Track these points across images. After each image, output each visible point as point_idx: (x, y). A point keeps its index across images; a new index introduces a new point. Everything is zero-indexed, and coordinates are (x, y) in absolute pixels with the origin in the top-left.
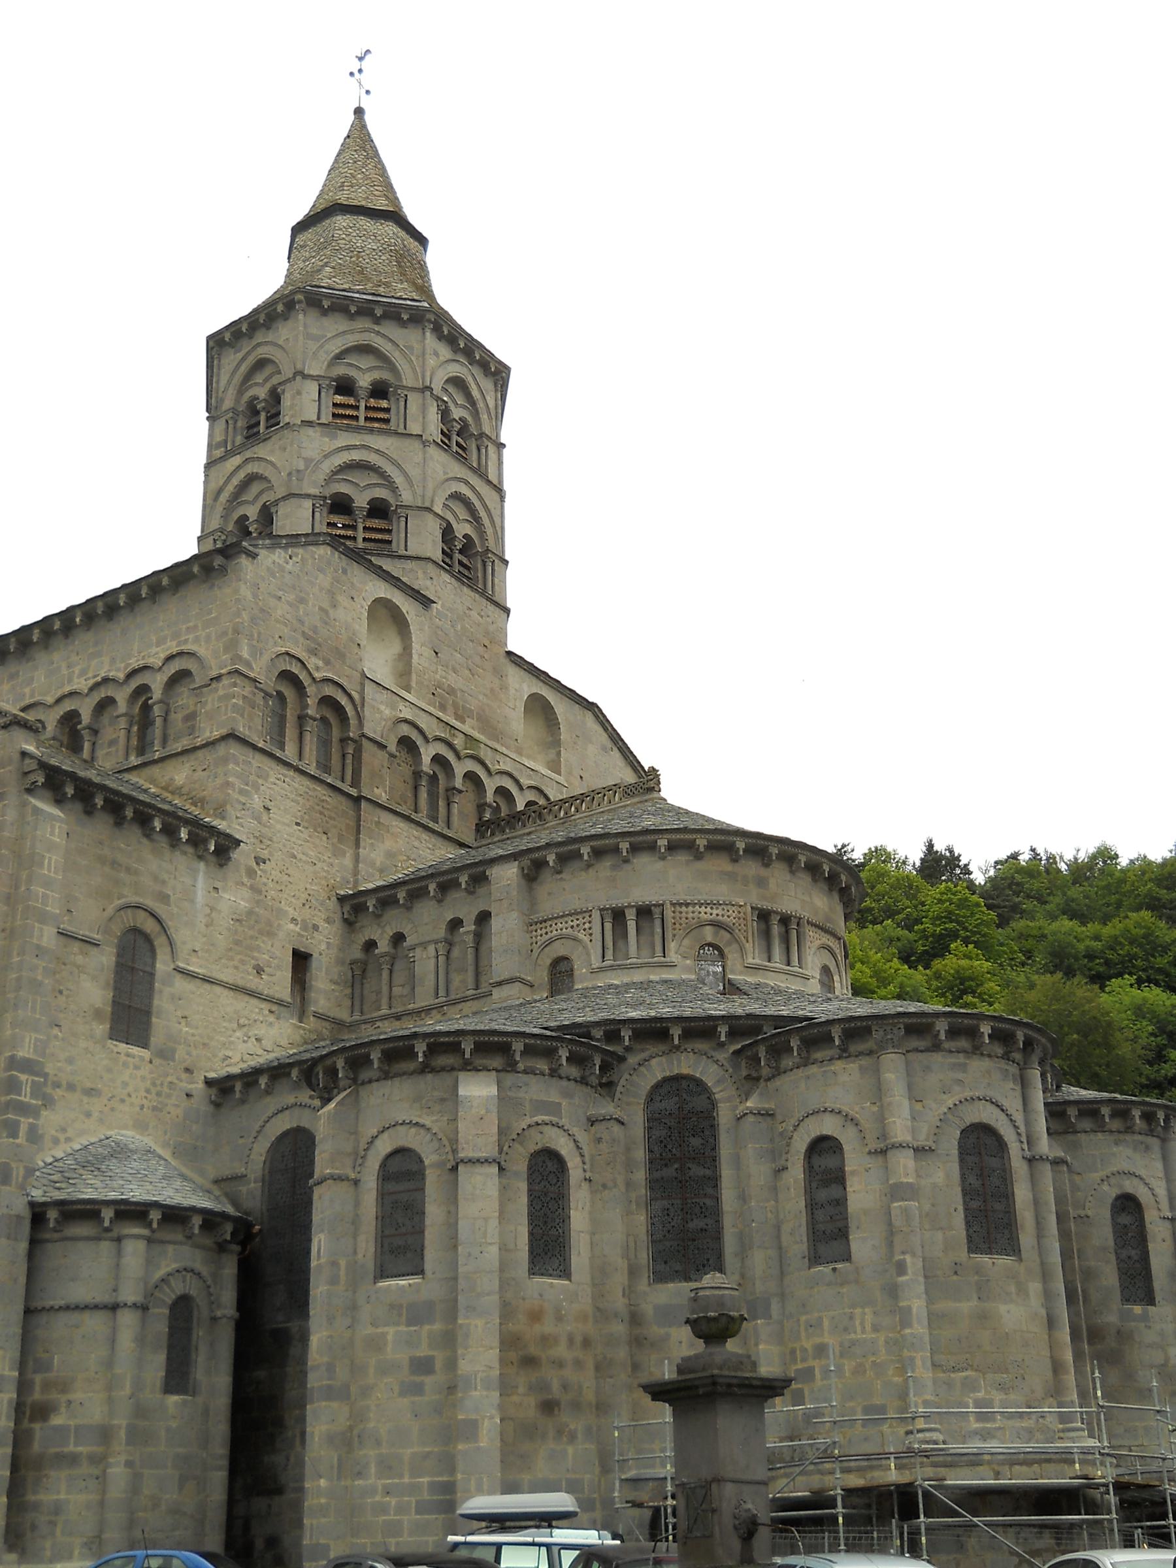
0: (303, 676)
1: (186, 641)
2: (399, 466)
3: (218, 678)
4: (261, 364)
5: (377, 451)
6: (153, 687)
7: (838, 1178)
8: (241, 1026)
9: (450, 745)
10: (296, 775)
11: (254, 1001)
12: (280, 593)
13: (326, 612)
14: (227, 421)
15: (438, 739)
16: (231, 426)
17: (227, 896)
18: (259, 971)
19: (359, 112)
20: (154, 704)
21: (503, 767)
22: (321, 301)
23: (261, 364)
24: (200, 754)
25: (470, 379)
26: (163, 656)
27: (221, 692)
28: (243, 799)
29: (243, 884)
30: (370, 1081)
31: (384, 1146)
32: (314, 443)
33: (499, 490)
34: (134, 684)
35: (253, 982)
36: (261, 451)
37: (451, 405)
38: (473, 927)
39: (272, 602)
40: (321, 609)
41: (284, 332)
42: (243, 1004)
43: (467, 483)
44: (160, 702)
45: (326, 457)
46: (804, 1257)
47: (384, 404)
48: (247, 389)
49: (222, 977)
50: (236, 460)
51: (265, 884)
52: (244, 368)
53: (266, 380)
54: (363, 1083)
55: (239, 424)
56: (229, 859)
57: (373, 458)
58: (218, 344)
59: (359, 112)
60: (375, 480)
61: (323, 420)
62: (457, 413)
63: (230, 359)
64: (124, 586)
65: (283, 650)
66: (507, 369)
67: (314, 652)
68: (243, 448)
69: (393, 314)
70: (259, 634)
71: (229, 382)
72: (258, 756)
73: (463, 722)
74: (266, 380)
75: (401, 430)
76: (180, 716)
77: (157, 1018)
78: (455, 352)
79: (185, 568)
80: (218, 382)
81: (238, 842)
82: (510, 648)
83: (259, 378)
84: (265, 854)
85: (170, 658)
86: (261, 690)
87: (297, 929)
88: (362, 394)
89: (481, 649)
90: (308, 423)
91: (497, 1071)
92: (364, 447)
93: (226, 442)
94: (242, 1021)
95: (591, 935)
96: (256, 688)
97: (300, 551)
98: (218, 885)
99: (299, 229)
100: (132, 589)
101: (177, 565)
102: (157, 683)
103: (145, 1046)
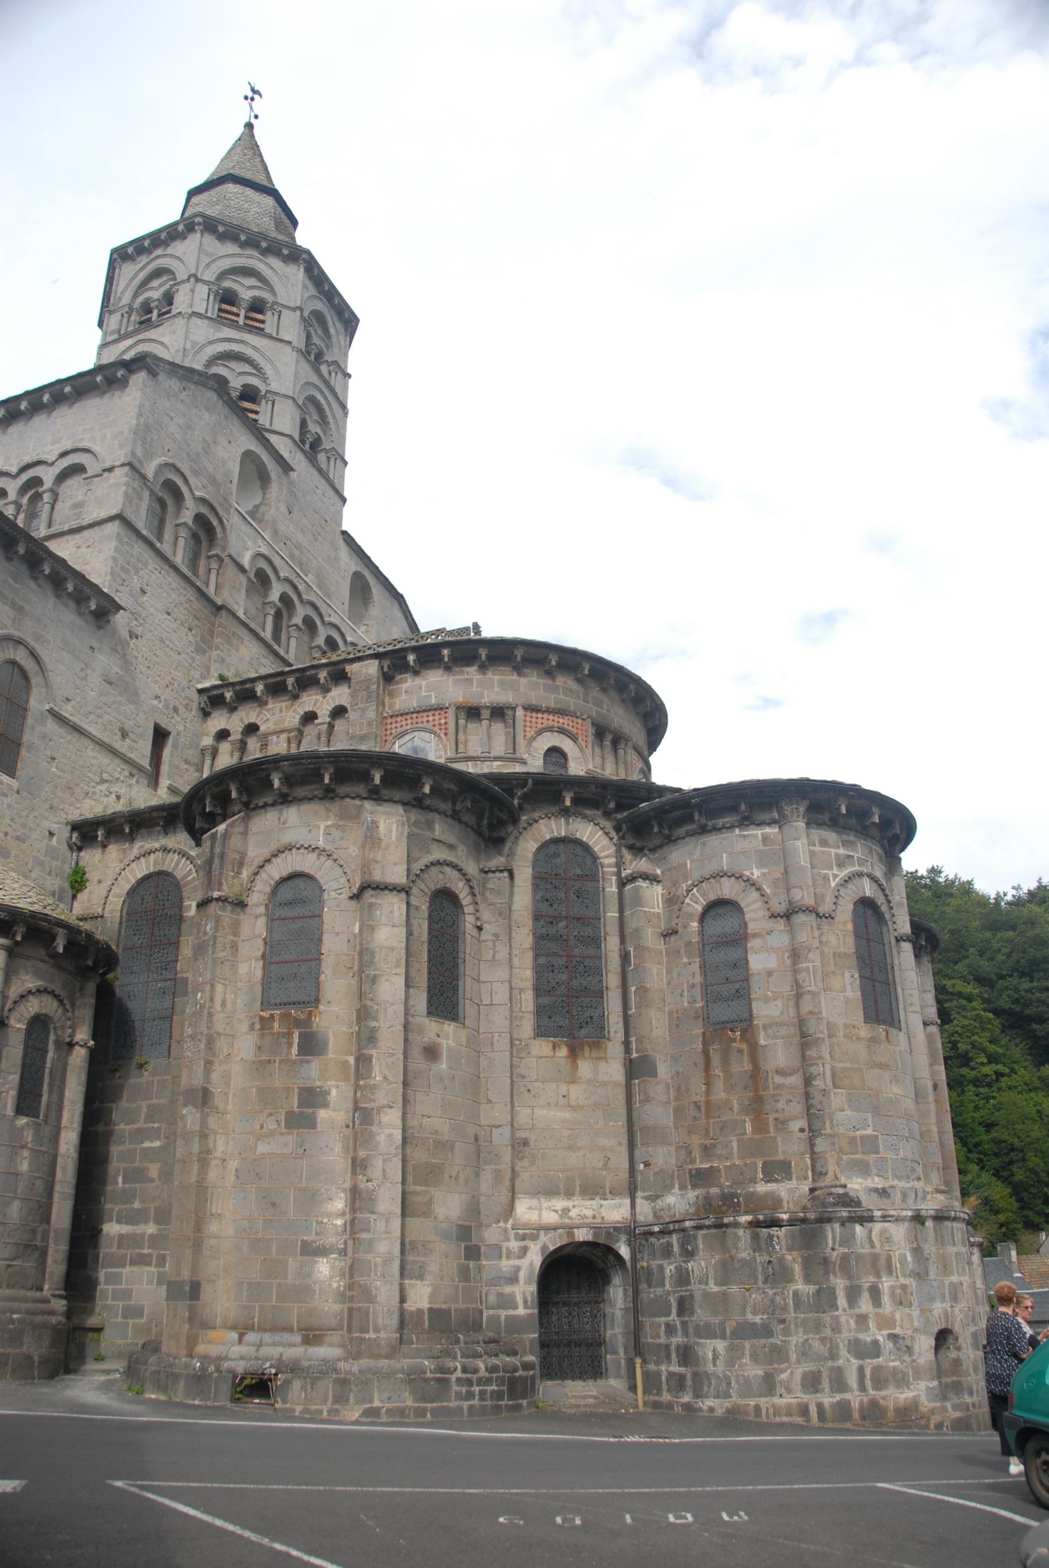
0: (184, 489)
1: (82, 440)
2: (270, 361)
3: (110, 470)
4: (158, 273)
5: (254, 347)
6: (44, 479)
7: (739, 939)
8: (103, 781)
9: (295, 588)
10: (171, 570)
11: (117, 761)
12: (172, 414)
13: (209, 445)
14: (122, 315)
15: (287, 580)
16: (125, 320)
17: (101, 657)
18: (124, 735)
19: (249, 126)
20: (45, 492)
21: (332, 620)
22: (216, 227)
23: (158, 273)
24: (86, 533)
25: (328, 317)
26: (56, 453)
27: (112, 481)
28: (123, 575)
29: (116, 651)
30: (265, 806)
31: (277, 870)
32: (202, 331)
33: (344, 407)
34: (25, 477)
35: (118, 745)
36: (152, 334)
37: (313, 335)
38: (328, 719)
39: (166, 419)
40: (204, 440)
41: (178, 248)
42: (107, 761)
43: (322, 392)
44: (51, 490)
45: (211, 343)
46: (698, 1017)
47: (260, 317)
48: (142, 293)
49: (92, 730)
50: (129, 342)
51: (137, 658)
52: (142, 276)
53: (161, 285)
54: (257, 807)
55: (133, 318)
56: (109, 621)
57: (249, 352)
58: (121, 256)
59: (249, 126)
60: (248, 369)
61: (209, 314)
62: (316, 340)
63: (127, 271)
64: (27, 393)
65: (171, 461)
66: (357, 320)
67: (195, 473)
68: (136, 332)
69: (273, 249)
70: (152, 440)
71: (128, 286)
72: (141, 543)
73: (306, 575)
74: (161, 285)
75: (274, 335)
76: (68, 504)
77: (28, 752)
78: (319, 293)
79: (88, 378)
80: (117, 286)
81: (119, 608)
82: (344, 528)
83: (155, 283)
84: (139, 630)
85: (64, 454)
86: (148, 487)
87: (161, 706)
88: (244, 305)
89: (323, 522)
90: (198, 315)
91: (404, 804)
92: (242, 342)
93: (119, 330)
94: (105, 776)
95: (446, 729)
96: (145, 484)
97: (193, 387)
98: (95, 645)
99: (193, 193)
100: (34, 396)
101: (81, 375)
102: (48, 476)
103: (12, 774)
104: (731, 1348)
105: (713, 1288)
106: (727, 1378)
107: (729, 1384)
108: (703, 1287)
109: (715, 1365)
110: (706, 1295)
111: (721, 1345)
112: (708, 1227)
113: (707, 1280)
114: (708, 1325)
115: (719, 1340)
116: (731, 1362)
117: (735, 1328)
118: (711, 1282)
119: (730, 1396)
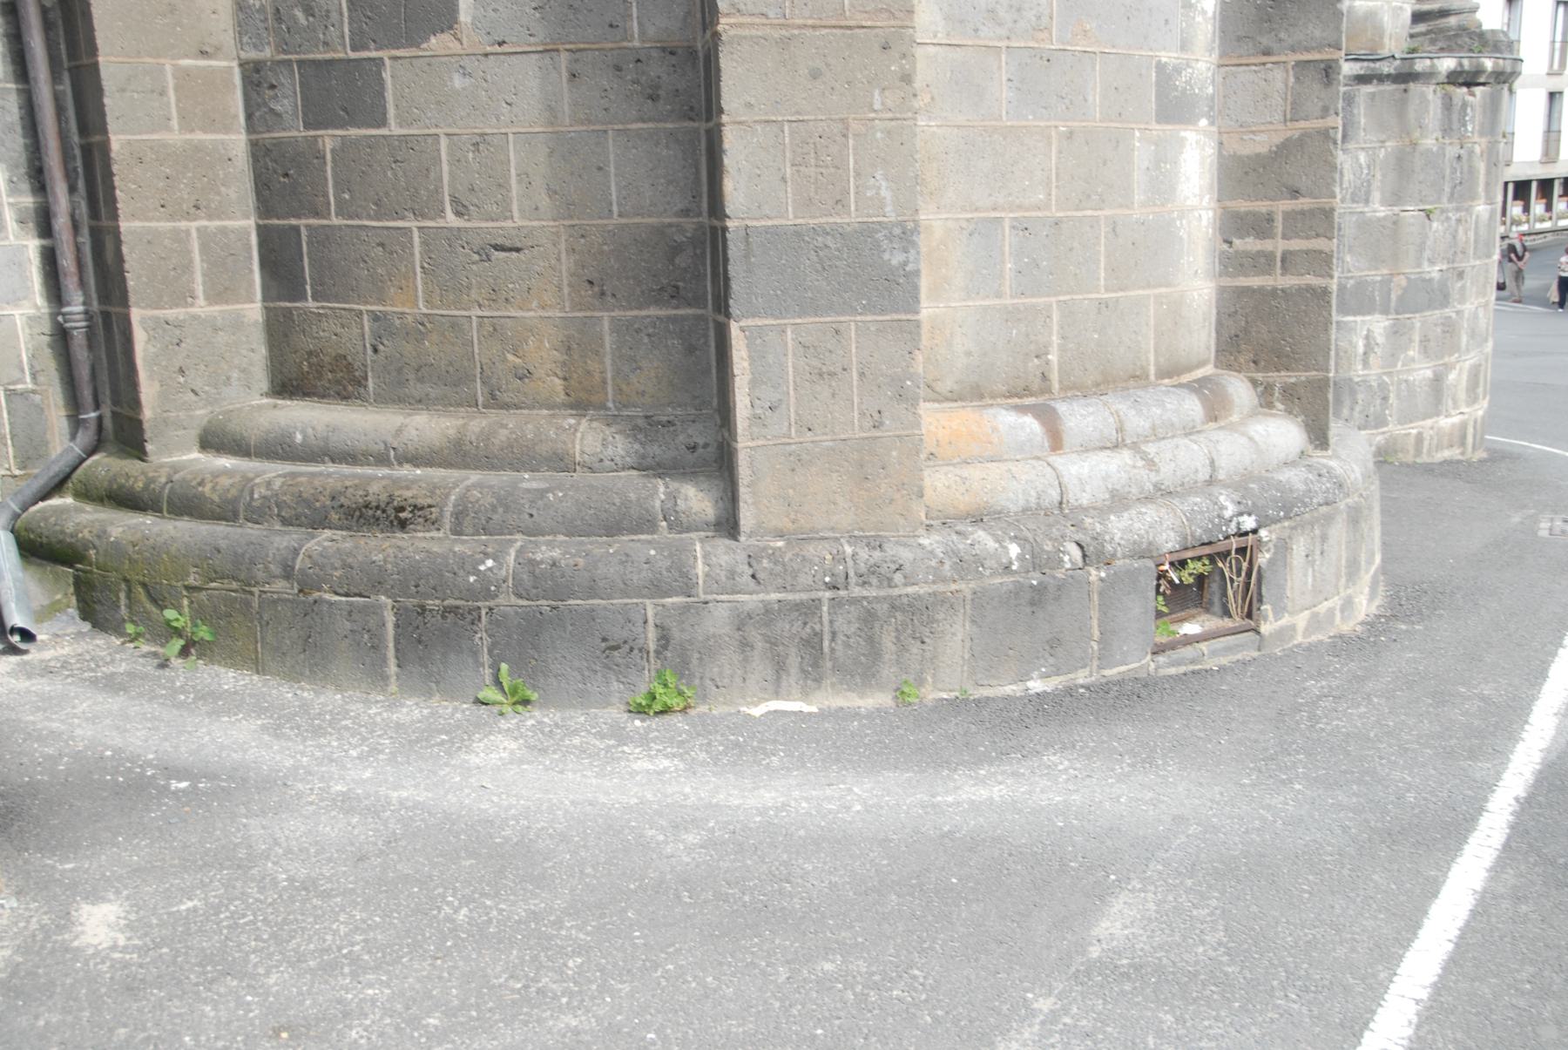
104: (1396, 332)
105: (1378, 209)
106: (1383, 386)
107: (1385, 399)
108: (1360, 207)
109: (1366, 364)
110: (1365, 224)
111: (1378, 325)
112: (1382, 78)
113: (1368, 193)
114: (1361, 284)
115: (1377, 316)
116: (1392, 357)
117: (1405, 290)
118: (1376, 196)
119: (1384, 423)
